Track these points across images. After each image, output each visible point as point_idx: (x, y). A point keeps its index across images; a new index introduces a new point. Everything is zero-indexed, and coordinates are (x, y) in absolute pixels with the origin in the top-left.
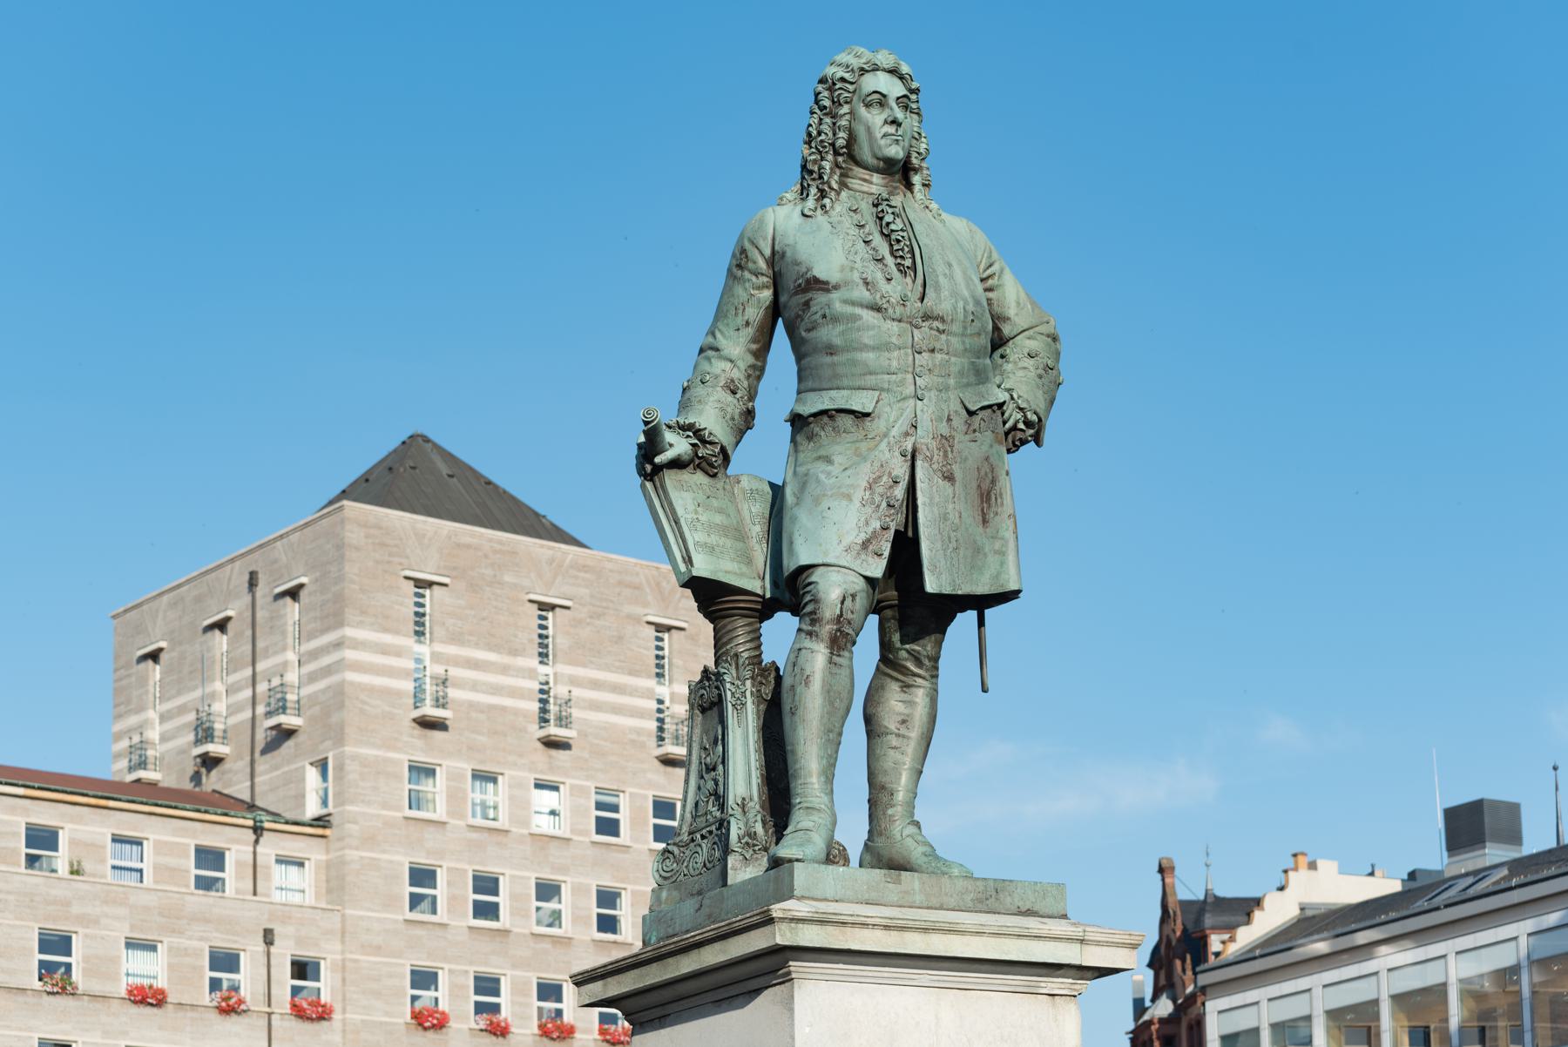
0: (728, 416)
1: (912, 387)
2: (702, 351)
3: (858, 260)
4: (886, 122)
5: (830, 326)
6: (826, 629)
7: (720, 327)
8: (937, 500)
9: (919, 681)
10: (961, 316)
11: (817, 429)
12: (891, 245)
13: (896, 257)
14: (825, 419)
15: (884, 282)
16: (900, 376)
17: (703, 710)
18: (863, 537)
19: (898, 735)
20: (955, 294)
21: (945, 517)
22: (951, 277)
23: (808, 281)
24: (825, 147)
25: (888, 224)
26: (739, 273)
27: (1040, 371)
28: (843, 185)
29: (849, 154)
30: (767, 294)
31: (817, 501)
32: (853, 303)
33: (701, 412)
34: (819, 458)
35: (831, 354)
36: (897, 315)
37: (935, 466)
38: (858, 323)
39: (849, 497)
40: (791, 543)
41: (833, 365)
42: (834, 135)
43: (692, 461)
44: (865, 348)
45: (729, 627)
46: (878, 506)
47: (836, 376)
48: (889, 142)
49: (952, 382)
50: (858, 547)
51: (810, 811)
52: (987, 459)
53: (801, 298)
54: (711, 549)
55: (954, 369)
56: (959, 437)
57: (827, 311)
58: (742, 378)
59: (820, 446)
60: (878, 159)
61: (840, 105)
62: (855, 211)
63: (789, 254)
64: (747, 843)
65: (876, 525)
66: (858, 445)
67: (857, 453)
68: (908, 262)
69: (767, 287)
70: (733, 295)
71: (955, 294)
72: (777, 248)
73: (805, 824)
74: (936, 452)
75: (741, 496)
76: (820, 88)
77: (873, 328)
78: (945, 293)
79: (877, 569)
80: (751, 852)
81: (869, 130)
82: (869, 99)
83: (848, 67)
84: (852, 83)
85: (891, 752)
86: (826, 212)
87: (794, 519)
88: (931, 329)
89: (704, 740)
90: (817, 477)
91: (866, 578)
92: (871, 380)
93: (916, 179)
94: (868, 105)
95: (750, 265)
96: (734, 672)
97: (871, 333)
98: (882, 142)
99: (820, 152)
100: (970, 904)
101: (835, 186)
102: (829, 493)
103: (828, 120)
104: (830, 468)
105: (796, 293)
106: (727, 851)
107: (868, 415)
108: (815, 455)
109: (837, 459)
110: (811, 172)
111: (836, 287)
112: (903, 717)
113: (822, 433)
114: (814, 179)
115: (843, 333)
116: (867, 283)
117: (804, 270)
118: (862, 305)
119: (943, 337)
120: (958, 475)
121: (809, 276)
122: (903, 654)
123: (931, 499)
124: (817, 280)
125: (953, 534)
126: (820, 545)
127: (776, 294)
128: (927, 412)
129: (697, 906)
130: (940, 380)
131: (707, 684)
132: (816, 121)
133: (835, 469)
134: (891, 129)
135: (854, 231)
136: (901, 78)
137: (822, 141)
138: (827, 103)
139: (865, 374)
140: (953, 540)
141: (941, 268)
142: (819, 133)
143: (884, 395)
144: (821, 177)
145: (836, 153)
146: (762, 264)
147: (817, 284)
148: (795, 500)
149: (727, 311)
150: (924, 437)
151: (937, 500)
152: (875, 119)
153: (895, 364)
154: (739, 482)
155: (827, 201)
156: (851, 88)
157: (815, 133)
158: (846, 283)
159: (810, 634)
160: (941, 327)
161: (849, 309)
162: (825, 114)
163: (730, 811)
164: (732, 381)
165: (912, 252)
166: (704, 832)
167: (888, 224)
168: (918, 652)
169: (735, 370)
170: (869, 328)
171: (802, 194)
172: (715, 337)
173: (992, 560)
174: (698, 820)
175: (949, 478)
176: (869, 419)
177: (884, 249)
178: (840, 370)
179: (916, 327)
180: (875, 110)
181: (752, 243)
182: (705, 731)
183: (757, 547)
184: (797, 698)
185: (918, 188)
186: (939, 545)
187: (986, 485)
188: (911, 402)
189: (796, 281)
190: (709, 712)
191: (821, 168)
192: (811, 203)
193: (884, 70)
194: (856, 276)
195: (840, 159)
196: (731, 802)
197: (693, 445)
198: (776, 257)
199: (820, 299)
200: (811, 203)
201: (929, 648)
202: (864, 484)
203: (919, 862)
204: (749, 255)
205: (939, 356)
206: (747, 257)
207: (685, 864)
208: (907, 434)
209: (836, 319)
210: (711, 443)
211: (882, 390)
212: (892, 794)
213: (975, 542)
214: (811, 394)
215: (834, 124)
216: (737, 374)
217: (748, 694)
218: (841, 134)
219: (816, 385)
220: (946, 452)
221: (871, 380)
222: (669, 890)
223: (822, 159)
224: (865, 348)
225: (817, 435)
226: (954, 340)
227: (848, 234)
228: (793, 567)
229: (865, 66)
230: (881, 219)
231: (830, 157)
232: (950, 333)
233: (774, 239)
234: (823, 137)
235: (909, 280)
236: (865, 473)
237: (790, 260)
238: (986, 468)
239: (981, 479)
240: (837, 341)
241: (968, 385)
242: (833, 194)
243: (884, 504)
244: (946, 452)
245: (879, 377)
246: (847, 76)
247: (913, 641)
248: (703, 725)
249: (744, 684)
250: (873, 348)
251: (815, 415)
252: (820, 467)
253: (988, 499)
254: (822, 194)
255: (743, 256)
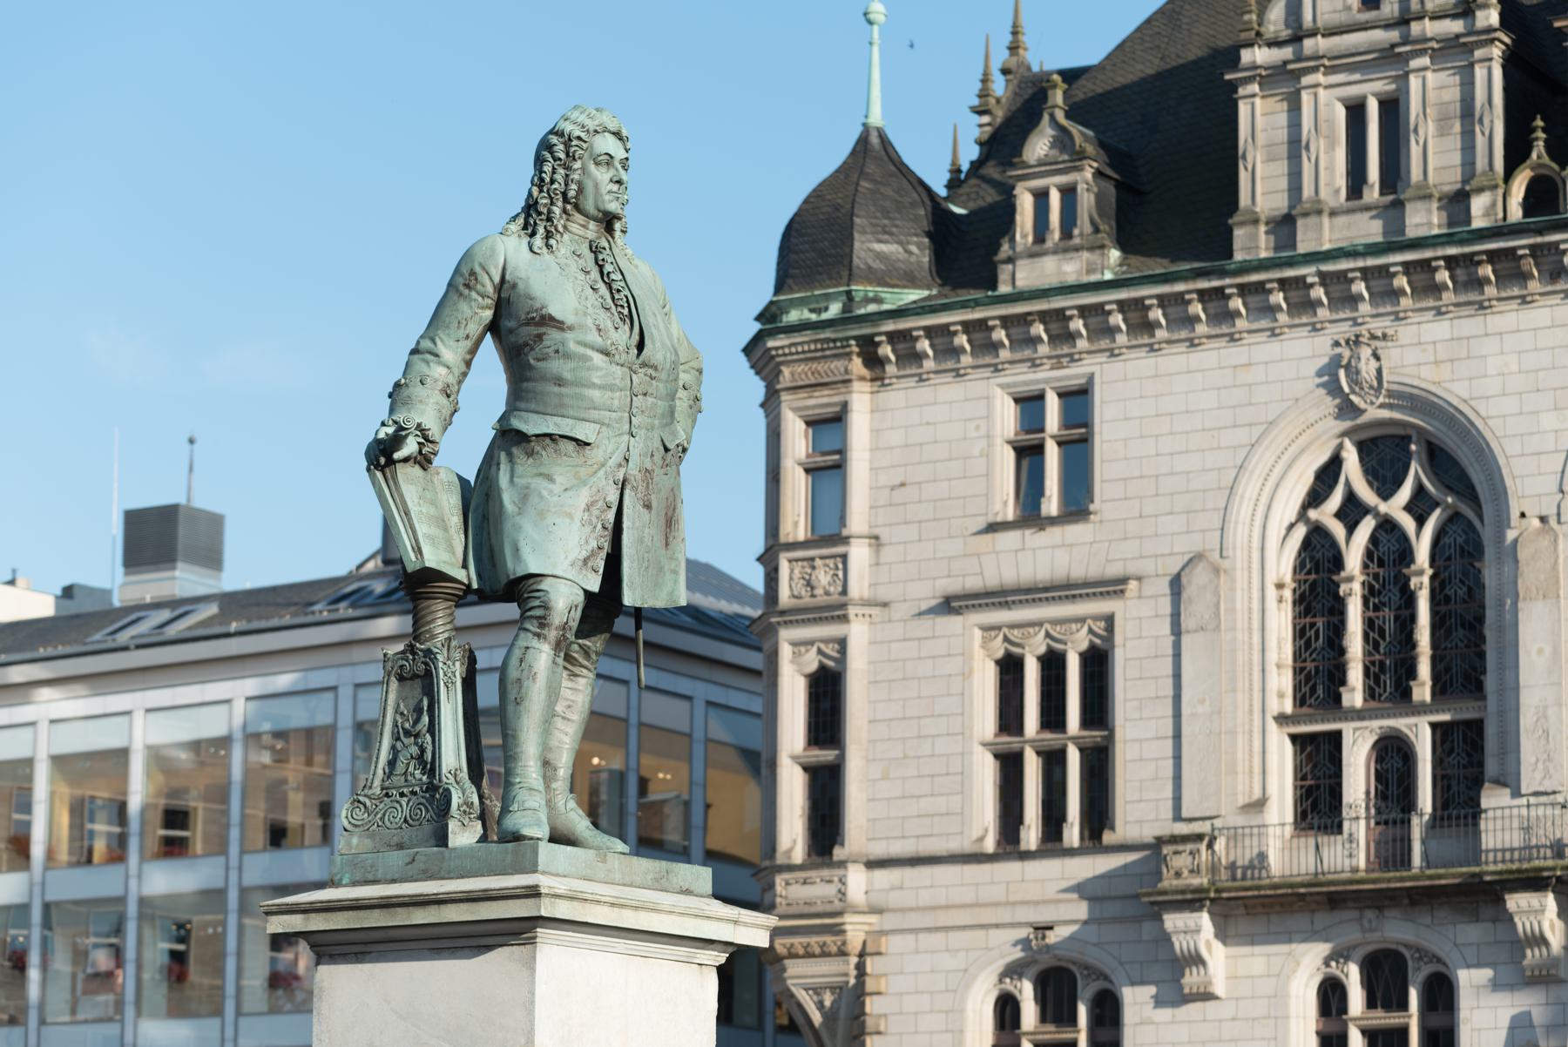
0: (443, 417)
1: (628, 426)
2: (415, 352)
3: (590, 306)
4: (611, 181)
5: (561, 361)
6: (553, 634)
7: (442, 335)
8: (637, 524)
9: (585, 671)
10: (668, 366)
11: (537, 448)
12: (611, 293)
13: (616, 305)
14: (548, 441)
15: (613, 330)
16: (619, 414)
17: (401, 679)
18: (584, 554)
19: (564, 718)
20: (663, 345)
21: (641, 540)
22: (657, 327)
23: (543, 317)
24: (557, 194)
25: (609, 273)
26: (466, 292)
27: (691, 402)
28: (565, 227)
29: (575, 205)
30: (488, 314)
31: (541, 515)
32: (585, 345)
33: (423, 413)
34: (541, 474)
35: (560, 385)
36: (622, 361)
37: (639, 495)
38: (588, 364)
39: (570, 516)
40: (516, 550)
41: (561, 395)
42: (566, 185)
43: (415, 458)
44: (593, 386)
45: (433, 608)
46: (595, 527)
47: (562, 405)
48: (611, 198)
49: (657, 422)
50: (581, 563)
51: (533, 792)
52: (672, 490)
53: (534, 330)
54: (432, 540)
55: (659, 411)
56: (658, 471)
57: (561, 348)
58: (455, 382)
59: (541, 465)
60: (599, 211)
61: (574, 159)
62: (579, 256)
63: (521, 286)
64: (465, 812)
65: (593, 544)
66: (578, 469)
67: (577, 476)
68: (626, 311)
69: (490, 308)
70: (457, 310)
71: (663, 345)
72: (507, 277)
73: (530, 804)
74: (641, 483)
75: (440, 487)
76: (554, 139)
77: (602, 369)
78: (658, 345)
79: (594, 585)
80: (467, 819)
81: (596, 186)
82: (600, 158)
83: (583, 127)
84: (585, 142)
85: (557, 732)
86: (552, 252)
87: (518, 528)
88: (646, 375)
89: (402, 706)
90: (540, 493)
91: (586, 592)
92: (594, 414)
93: (617, 226)
94: (597, 164)
95: (479, 287)
96: (445, 652)
97: (599, 374)
98: (607, 198)
99: (551, 198)
100: (650, 883)
101: (560, 229)
102: (553, 510)
103: (562, 171)
104: (551, 486)
105: (527, 324)
106: (443, 810)
107: (589, 444)
108: (535, 471)
109: (559, 479)
110: (540, 213)
111: (571, 328)
112: (569, 703)
113: (544, 453)
114: (541, 220)
115: (574, 370)
116: (600, 330)
117: (538, 305)
118: (593, 348)
119: (654, 382)
120: (654, 504)
121: (544, 312)
122: (575, 647)
123: (633, 523)
124: (552, 318)
125: (646, 555)
126: (549, 557)
127: (495, 315)
128: (637, 447)
129: (408, 860)
130: (650, 420)
131: (411, 657)
132: (550, 169)
133: (557, 488)
134: (615, 187)
135: (581, 276)
136: (621, 139)
137: (555, 189)
138: (562, 156)
139: (589, 409)
140: (646, 560)
141: (651, 320)
142: (552, 181)
143: (604, 429)
144: (549, 219)
145: (566, 200)
146: (490, 289)
147: (548, 321)
148: (516, 510)
149: (450, 323)
150: (633, 469)
151: (637, 524)
152: (602, 176)
153: (616, 403)
154: (438, 474)
155: (552, 242)
156: (585, 146)
157: (548, 180)
158: (581, 326)
159: (538, 636)
160: (654, 375)
161: (581, 350)
162: (559, 165)
163: (444, 779)
164: (448, 386)
165: (628, 301)
166: (405, 790)
167: (609, 273)
168: (589, 648)
169: (451, 376)
170: (598, 369)
171: (525, 228)
172: (435, 344)
173: (668, 577)
174: (393, 778)
175: (648, 506)
176: (589, 448)
177: (609, 301)
178: (567, 401)
179: (635, 373)
180: (603, 169)
181: (484, 269)
182: (401, 697)
183: (455, 536)
184: (523, 690)
185: (618, 234)
186: (635, 564)
187: (669, 514)
188: (626, 437)
189: (528, 313)
190: (409, 683)
191: (550, 211)
192: (538, 241)
193: (610, 132)
194: (589, 322)
195: (569, 207)
196: (444, 771)
197: (419, 443)
198: (506, 286)
199: (553, 336)
200: (538, 241)
201: (598, 645)
202: (583, 506)
203: (583, 834)
204: (479, 278)
205: (650, 400)
206: (476, 279)
207: (379, 816)
208: (620, 465)
209: (568, 356)
210: (432, 442)
211: (603, 424)
212: (556, 770)
213: (660, 562)
214: (535, 416)
215: (567, 175)
216: (452, 380)
217: (458, 674)
218: (574, 187)
219: (541, 408)
220: (648, 483)
221: (594, 414)
222: (360, 837)
223: (552, 203)
224: (593, 386)
225: (538, 453)
226: (661, 386)
227: (576, 278)
228: (520, 572)
229: (598, 128)
230: (601, 267)
231: (560, 204)
232: (659, 380)
233: (504, 269)
234: (554, 186)
235: (627, 328)
236: (583, 496)
237: (522, 293)
238: (671, 499)
239: (667, 507)
240: (567, 375)
241: (666, 425)
242: (559, 236)
243: (599, 526)
244: (648, 483)
245: (602, 412)
246: (583, 135)
247: (586, 637)
248: (399, 692)
249: (454, 664)
250: (600, 387)
251: (537, 436)
252: (541, 484)
253: (671, 525)
254: (548, 235)
255: (472, 278)
